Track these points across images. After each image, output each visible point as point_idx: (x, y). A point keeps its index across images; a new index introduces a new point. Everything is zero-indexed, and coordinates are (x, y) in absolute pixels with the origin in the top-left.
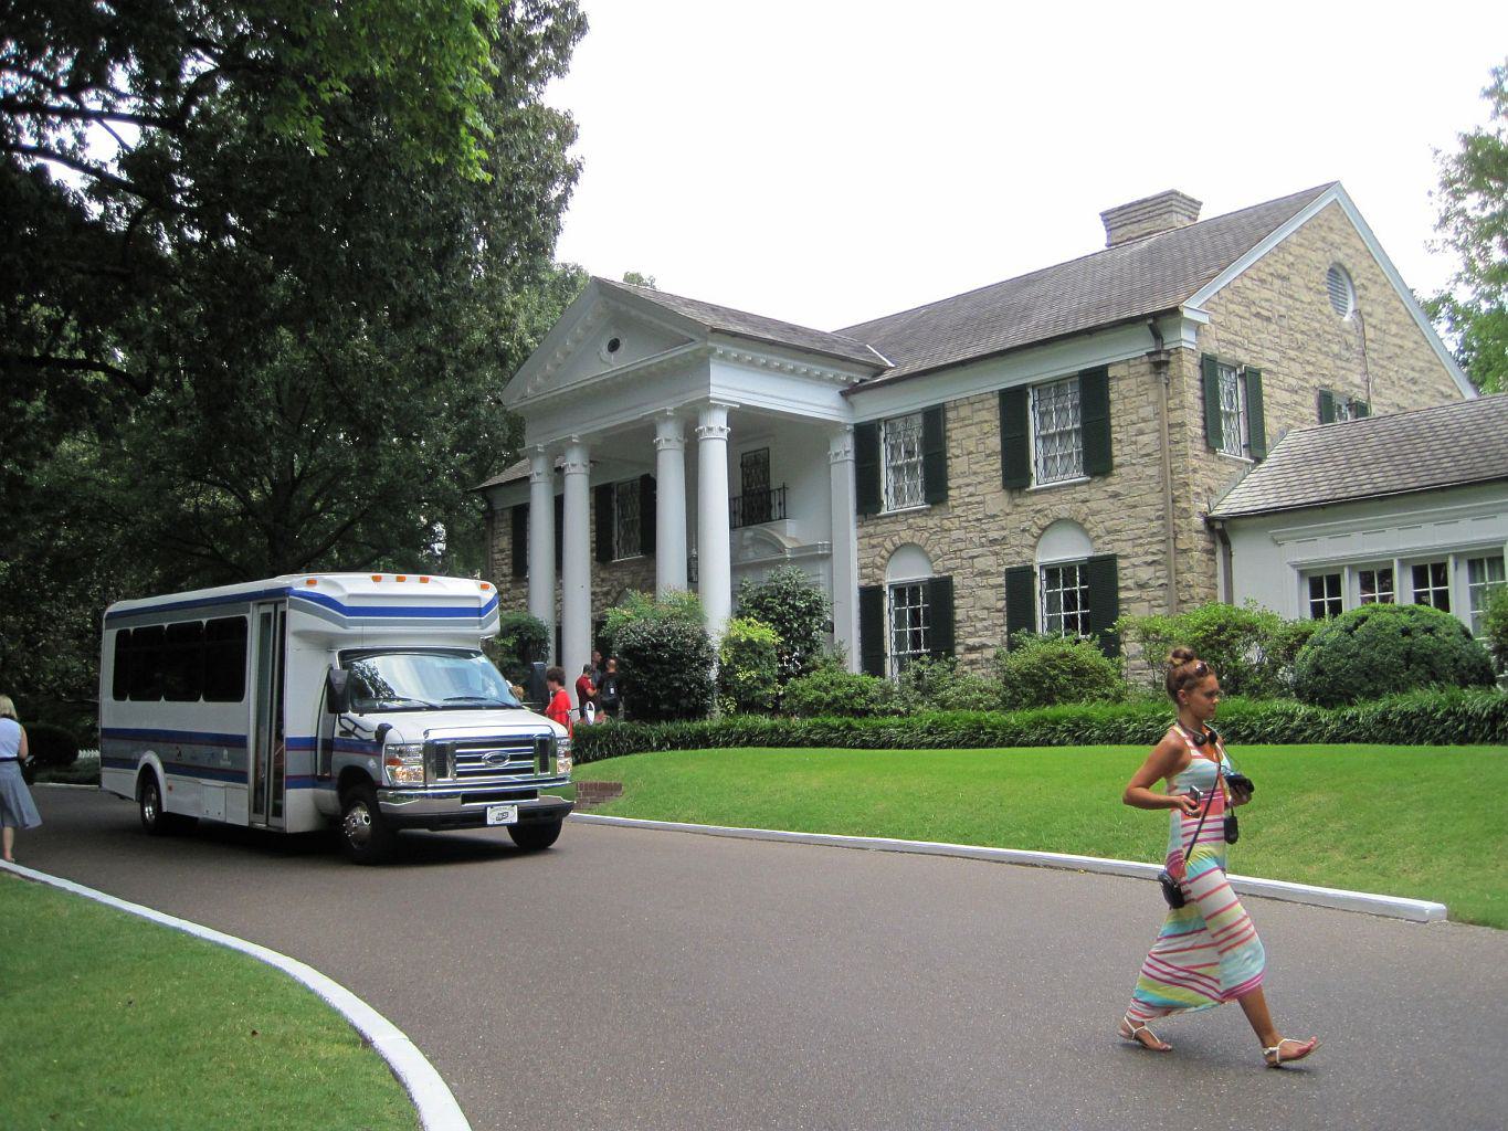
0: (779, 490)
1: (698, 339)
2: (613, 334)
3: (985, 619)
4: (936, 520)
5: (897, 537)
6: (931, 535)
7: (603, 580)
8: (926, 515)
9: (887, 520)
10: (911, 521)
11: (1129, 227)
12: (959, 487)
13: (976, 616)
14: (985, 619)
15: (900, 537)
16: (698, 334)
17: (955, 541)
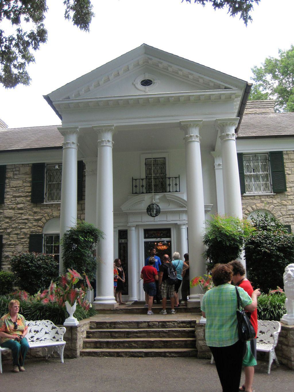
0: (176, 178)
1: (234, 88)
2: (147, 77)
4: (278, 200)
5: (255, 206)
6: (275, 206)
7: (35, 213)
8: (272, 198)
9: (248, 198)
10: (263, 199)
11: (255, 109)
12: (291, 187)
15: (256, 206)
16: (236, 87)
17: (289, 210)
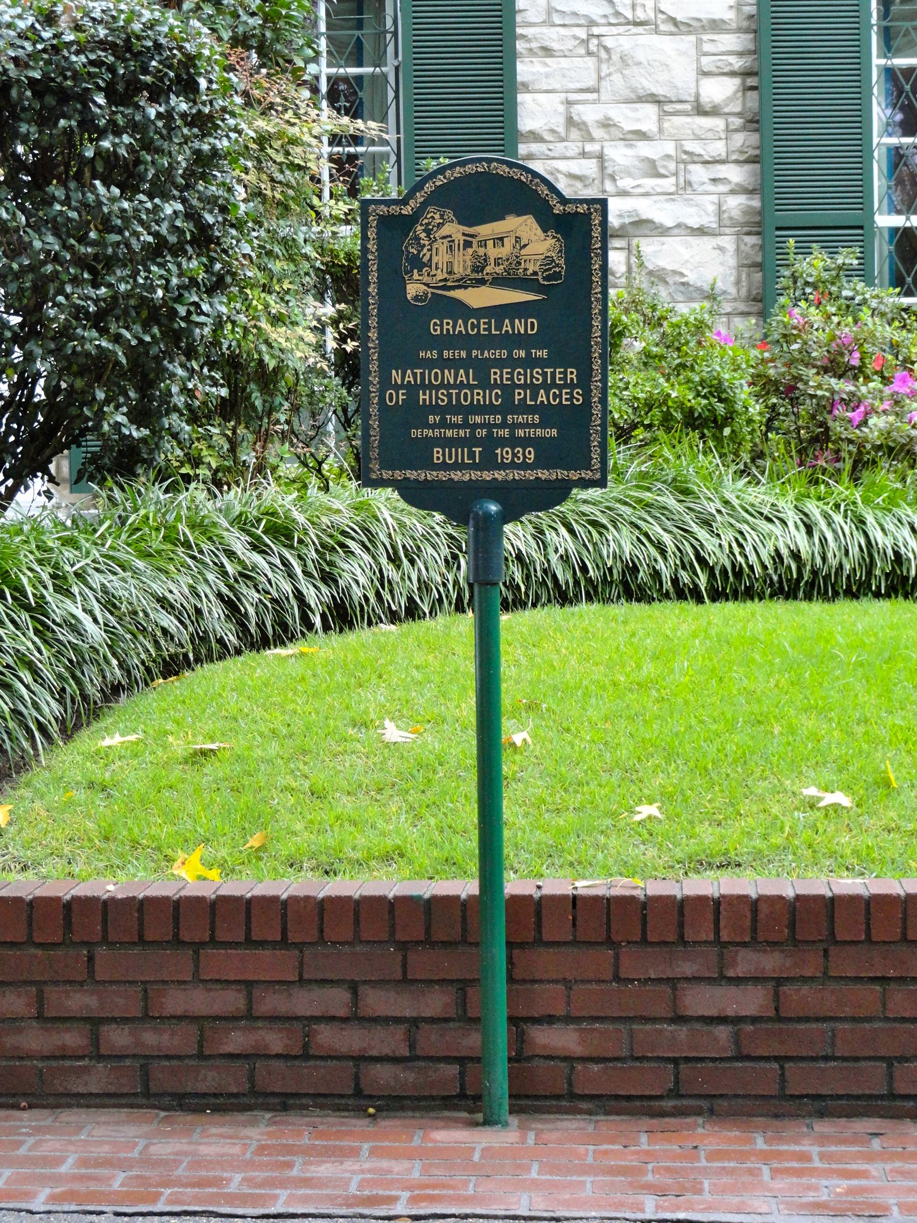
3: (642, 135)
13: (606, 124)
14: (642, 135)
